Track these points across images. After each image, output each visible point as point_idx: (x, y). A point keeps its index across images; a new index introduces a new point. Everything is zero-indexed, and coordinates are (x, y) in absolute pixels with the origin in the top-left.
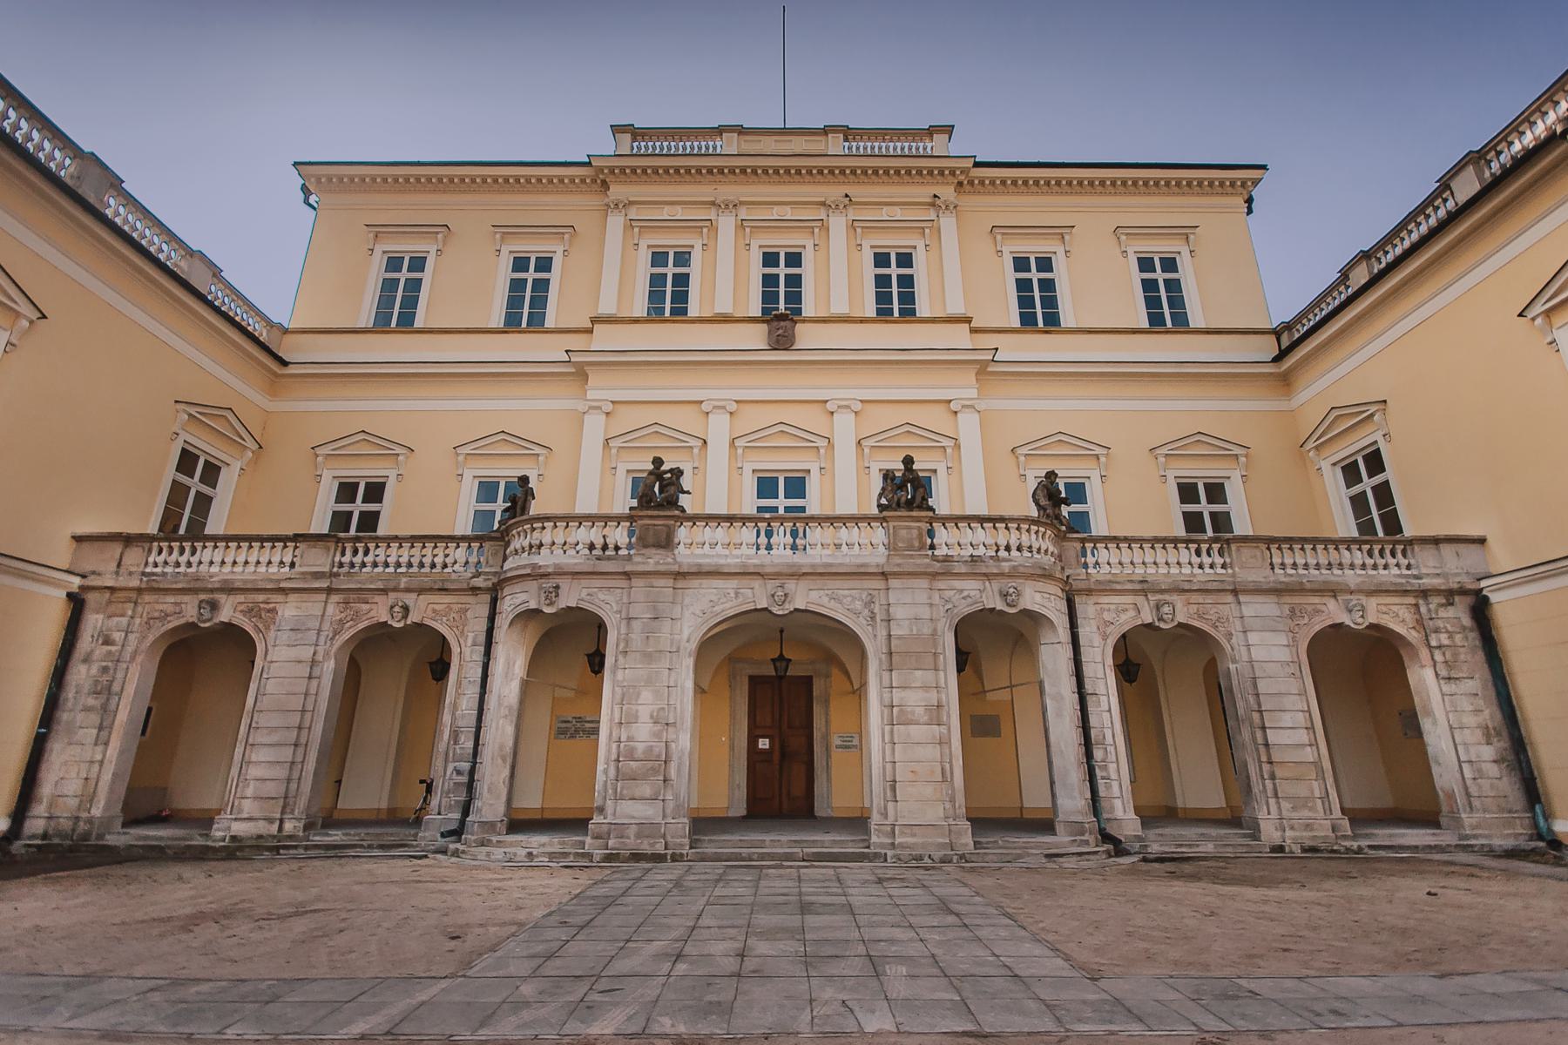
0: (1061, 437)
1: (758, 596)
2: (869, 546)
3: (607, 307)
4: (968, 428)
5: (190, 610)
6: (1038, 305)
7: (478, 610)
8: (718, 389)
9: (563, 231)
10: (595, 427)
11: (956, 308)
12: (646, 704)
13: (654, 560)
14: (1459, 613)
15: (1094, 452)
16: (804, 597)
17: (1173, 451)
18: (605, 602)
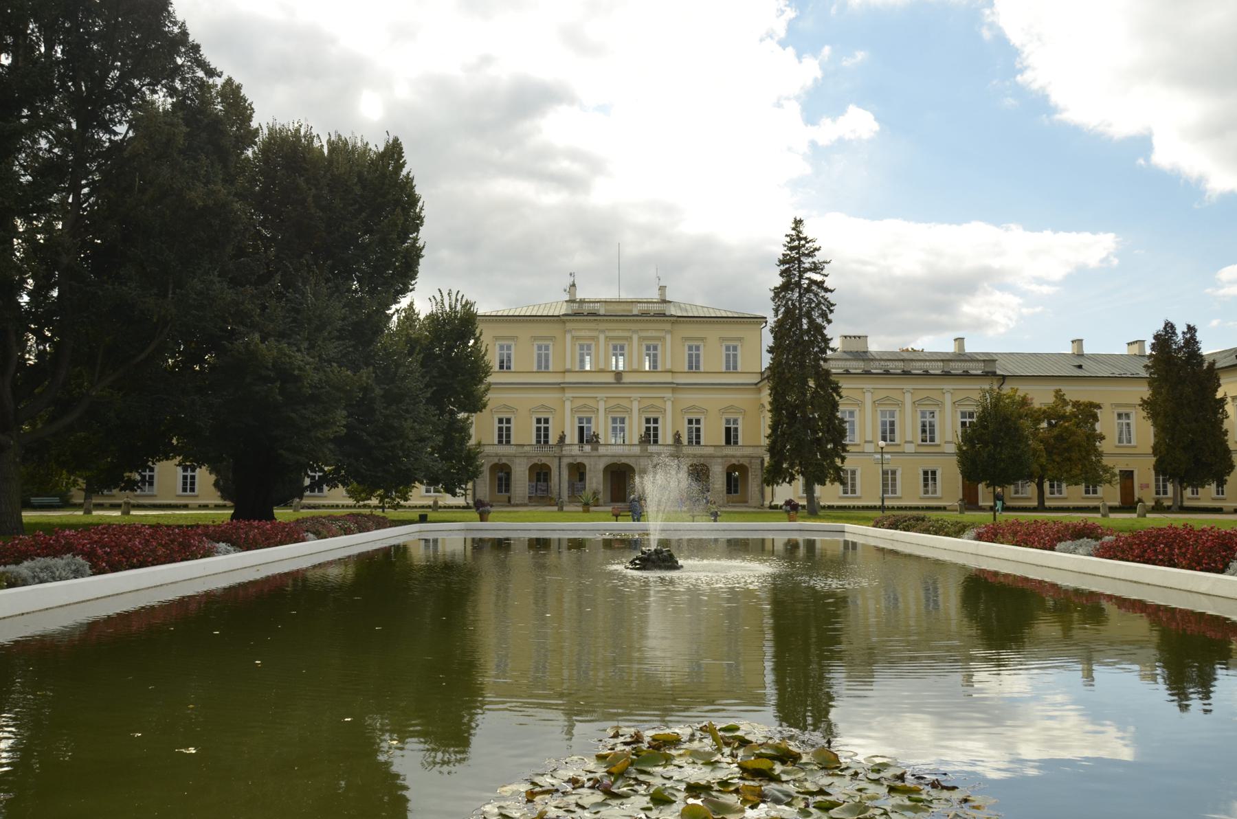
0: (693, 407)
1: (615, 460)
2: (637, 450)
3: (568, 366)
4: (669, 404)
5: (496, 460)
6: (694, 365)
7: (557, 460)
8: (601, 395)
9: (552, 338)
10: (568, 405)
11: (668, 367)
12: (594, 480)
13: (595, 453)
14: (759, 461)
15: (704, 411)
16: (624, 460)
17: (724, 411)
18: (586, 461)
